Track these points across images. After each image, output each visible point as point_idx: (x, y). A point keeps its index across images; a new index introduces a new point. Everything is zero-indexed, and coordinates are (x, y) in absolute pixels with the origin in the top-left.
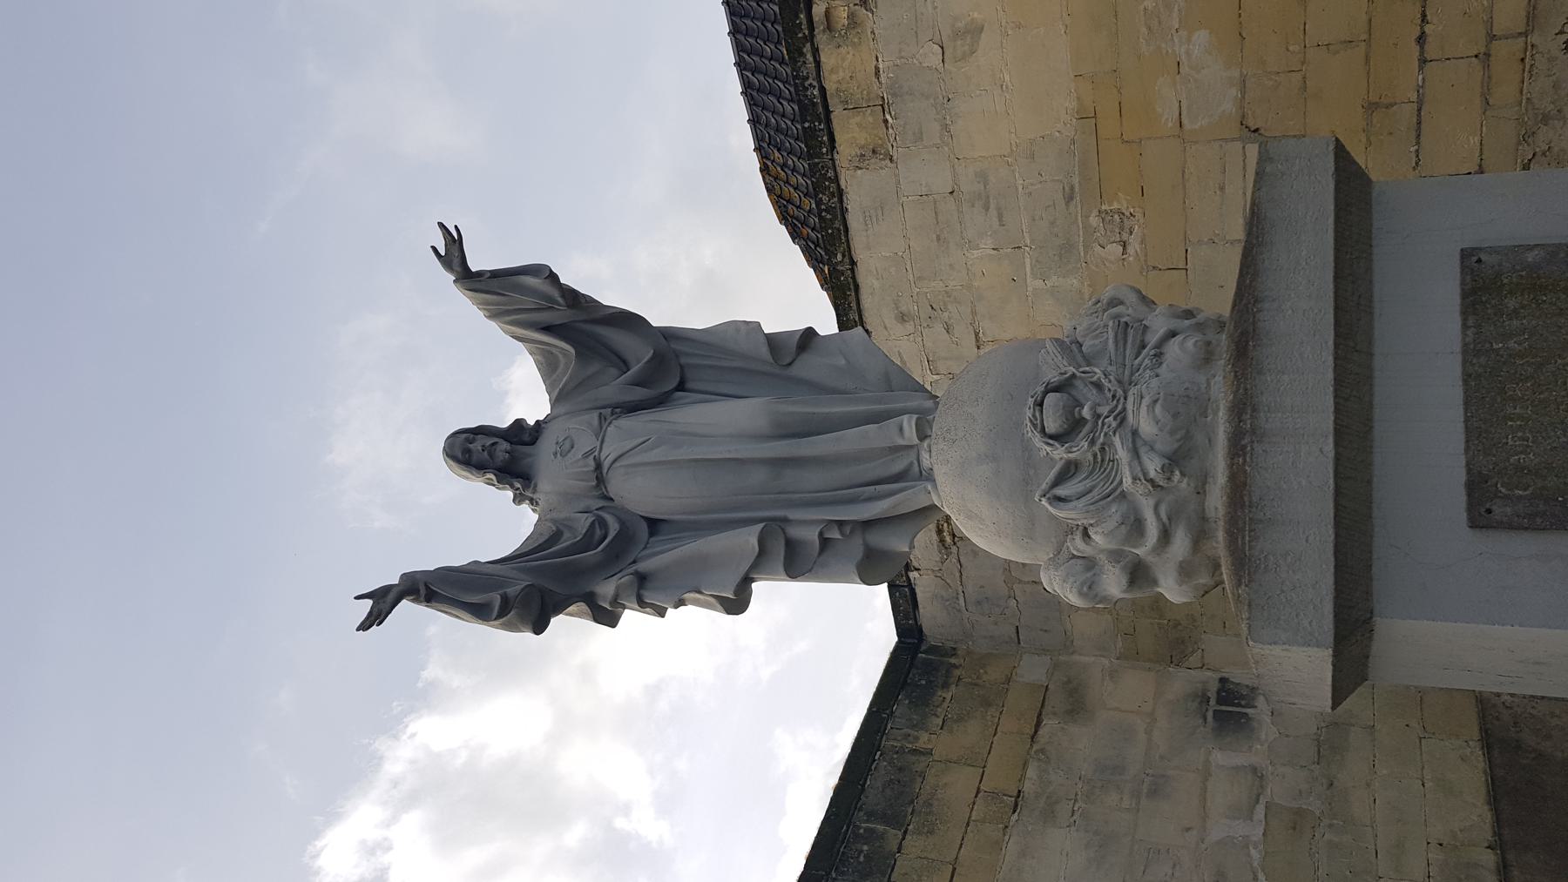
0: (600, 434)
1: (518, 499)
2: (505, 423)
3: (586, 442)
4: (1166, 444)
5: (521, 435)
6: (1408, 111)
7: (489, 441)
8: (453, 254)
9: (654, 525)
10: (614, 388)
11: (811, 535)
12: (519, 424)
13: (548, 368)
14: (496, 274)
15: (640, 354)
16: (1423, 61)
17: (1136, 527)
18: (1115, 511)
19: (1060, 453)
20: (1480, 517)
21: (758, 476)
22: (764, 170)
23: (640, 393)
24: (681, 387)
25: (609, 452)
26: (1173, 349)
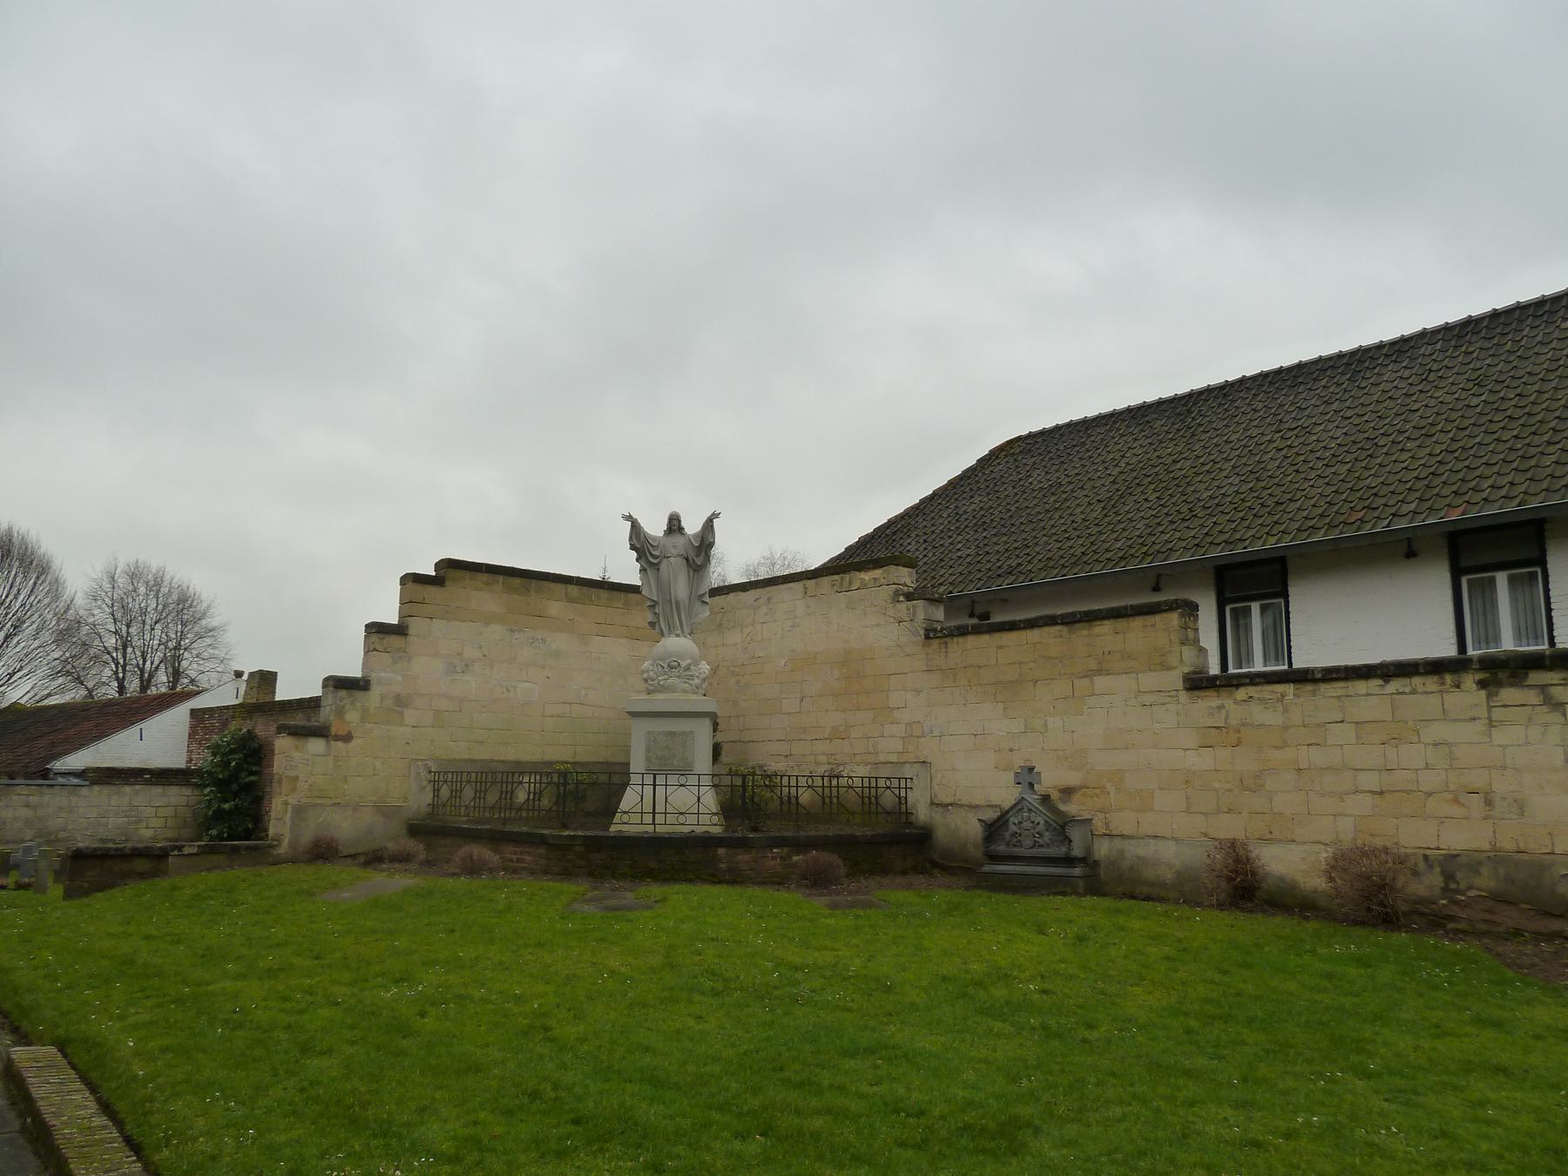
0: (679, 555)
1: (665, 531)
2: (683, 524)
3: (675, 552)
4: (666, 685)
5: (681, 529)
6: (802, 737)
7: (677, 524)
8: (715, 516)
9: (659, 569)
10: (691, 554)
11: (657, 611)
12: (683, 529)
13: (695, 536)
14: (712, 526)
15: (699, 561)
16: (812, 740)
17: (652, 680)
18: (655, 676)
19: (665, 666)
20: (649, 733)
21: (668, 598)
22: (1019, 439)
23: (691, 561)
24: (694, 570)
25: (672, 559)
26: (687, 685)
